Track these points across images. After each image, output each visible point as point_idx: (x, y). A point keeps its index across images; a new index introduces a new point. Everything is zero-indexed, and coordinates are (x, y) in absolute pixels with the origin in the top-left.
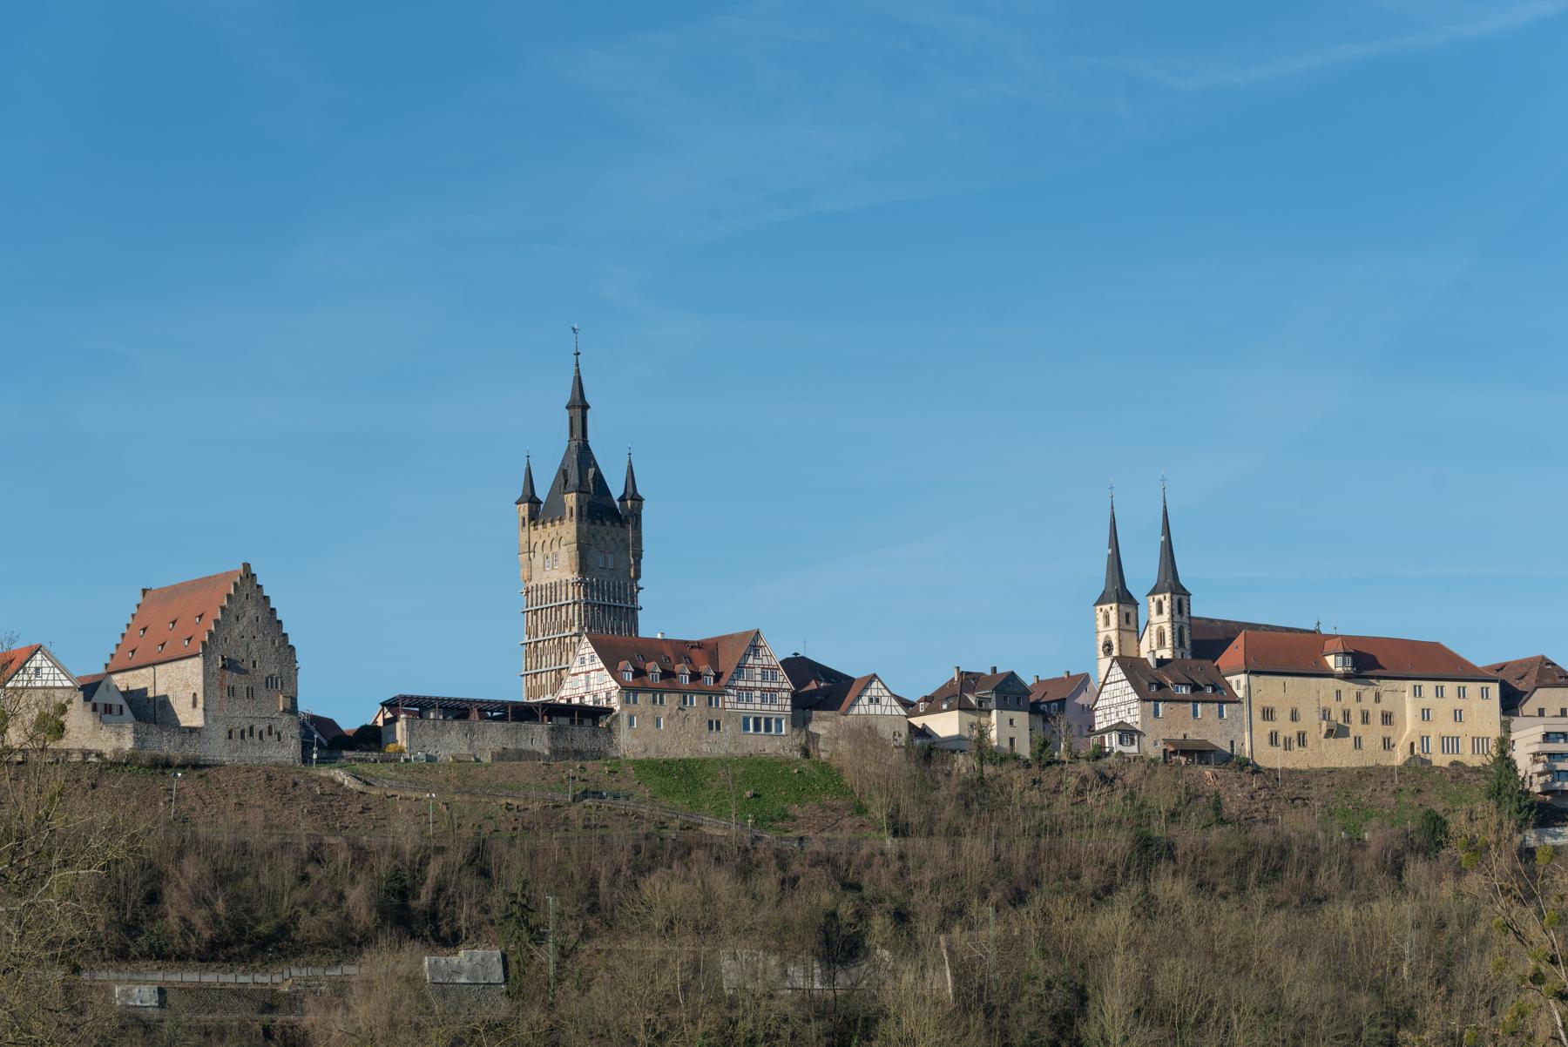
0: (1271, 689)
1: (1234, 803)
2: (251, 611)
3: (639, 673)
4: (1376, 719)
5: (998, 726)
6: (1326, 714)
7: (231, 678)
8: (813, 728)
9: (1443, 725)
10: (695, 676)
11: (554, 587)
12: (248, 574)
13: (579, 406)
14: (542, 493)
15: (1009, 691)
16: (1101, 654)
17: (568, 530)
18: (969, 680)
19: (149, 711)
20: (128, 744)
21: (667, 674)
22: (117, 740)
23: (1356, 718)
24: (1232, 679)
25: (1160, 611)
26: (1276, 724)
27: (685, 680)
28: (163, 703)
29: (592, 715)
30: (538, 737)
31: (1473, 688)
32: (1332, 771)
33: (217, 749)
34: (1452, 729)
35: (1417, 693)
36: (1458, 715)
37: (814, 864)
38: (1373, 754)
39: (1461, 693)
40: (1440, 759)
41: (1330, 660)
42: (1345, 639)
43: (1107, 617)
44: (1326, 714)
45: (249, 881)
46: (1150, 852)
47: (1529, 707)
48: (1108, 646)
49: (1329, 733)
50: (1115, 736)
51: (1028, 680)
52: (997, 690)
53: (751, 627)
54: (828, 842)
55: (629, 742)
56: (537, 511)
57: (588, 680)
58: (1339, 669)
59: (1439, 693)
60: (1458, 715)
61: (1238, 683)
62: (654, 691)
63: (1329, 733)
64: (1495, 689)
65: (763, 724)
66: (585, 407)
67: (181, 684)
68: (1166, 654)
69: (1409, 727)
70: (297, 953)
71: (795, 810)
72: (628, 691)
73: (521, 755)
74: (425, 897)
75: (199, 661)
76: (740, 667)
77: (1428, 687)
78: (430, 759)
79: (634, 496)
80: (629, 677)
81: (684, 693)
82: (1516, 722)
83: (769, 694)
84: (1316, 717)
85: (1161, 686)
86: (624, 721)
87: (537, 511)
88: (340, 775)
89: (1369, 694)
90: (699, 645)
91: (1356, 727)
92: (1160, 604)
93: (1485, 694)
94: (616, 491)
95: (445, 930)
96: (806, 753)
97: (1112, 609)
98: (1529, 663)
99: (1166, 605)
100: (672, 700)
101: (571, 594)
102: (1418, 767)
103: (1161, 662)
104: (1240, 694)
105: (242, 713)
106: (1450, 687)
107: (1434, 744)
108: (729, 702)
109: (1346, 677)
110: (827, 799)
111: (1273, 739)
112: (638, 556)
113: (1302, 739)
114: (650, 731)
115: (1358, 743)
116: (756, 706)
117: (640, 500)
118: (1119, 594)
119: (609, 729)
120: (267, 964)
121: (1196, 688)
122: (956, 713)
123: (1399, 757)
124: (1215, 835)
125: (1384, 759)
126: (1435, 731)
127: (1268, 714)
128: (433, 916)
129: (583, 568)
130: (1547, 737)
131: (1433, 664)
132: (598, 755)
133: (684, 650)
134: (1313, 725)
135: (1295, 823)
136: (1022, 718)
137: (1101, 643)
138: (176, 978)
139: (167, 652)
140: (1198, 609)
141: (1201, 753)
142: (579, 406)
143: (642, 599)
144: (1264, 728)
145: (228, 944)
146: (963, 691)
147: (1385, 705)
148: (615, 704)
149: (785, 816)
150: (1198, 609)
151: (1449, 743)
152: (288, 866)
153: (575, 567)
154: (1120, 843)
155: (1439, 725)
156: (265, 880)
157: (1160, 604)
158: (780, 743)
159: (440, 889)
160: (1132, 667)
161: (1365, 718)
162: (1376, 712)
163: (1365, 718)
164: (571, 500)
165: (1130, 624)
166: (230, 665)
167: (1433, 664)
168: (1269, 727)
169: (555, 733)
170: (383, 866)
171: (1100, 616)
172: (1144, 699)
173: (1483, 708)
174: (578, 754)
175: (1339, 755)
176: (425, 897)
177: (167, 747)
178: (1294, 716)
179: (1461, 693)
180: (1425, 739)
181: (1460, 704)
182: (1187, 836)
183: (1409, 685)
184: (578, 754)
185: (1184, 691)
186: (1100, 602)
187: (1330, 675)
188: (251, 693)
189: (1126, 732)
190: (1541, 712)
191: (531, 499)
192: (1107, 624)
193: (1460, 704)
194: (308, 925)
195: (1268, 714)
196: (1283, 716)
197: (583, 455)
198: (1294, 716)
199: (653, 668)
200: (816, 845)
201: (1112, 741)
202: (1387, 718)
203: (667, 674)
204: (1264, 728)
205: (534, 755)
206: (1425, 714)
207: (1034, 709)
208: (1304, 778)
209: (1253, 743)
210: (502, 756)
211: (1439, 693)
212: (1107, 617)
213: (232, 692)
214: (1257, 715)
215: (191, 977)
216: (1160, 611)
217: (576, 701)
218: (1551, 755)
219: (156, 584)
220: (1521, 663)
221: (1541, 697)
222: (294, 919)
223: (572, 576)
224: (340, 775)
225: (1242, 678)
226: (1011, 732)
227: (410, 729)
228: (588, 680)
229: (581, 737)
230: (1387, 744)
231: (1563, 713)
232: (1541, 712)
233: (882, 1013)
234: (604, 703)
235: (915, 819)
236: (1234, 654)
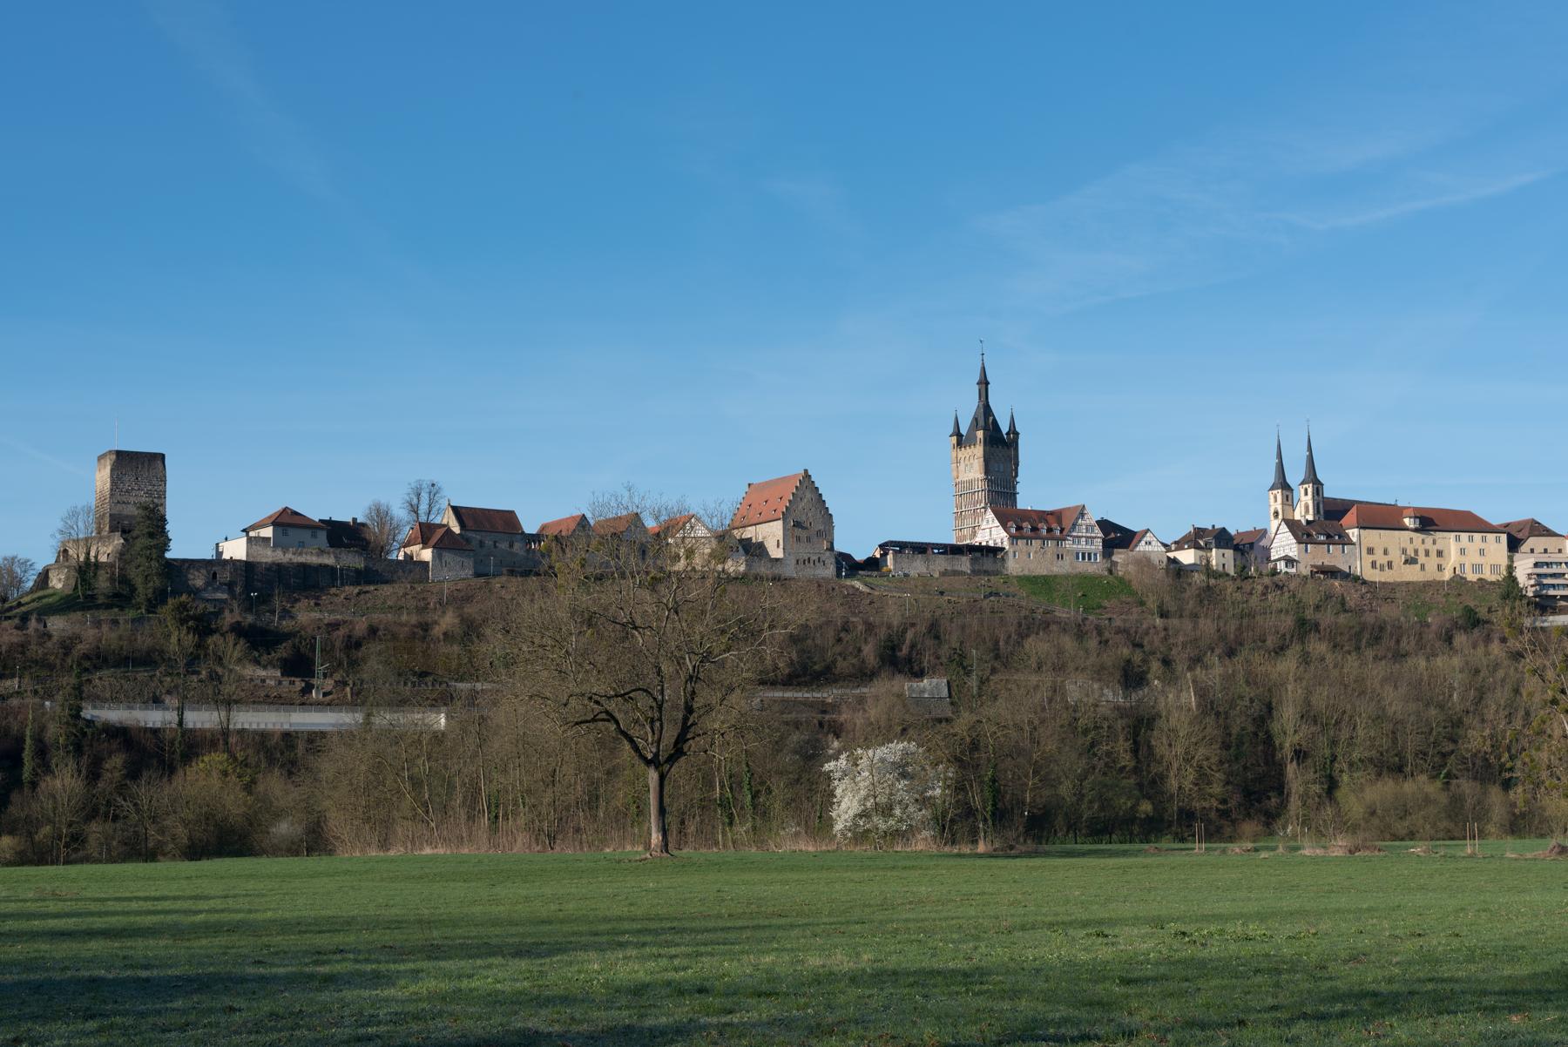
0: (1373, 537)
1: (1353, 598)
2: (808, 495)
3: (1019, 528)
4: (1433, 554)
5: (1215, 557)
6: (1404, 551)
7: (798, 531)
8: (1115, 558)
9: (1473, 558)
10: (1050, 530)
11: (971, 482)
12: (807, 475)
13: (984, 383)
14: (964, 431)
15: (1222, 538)
17: (979, 450)
18: (1199, 533)
19: (754, 550)
20: (742, 568)
21: (1035, 529)
22: (736, 565)
26: (1372, 556)
27: (1044, 532)
28: (761, 546)
29: (993, 551)
30: (964, 564)
31: (1491, 537)
32: (1408, 583)
33: (789, 570)
34: (1478, 560)
35: (1458, 539)
36: (1482, 552)
37: (1117, 633)
38: (1431, 574)
39: (1484, 540)
40: (1471, 577)
41: (1406, 521)
42: (1415, 509)
44: (1404, 551)
45: (809, 642)
46: (1305, 628)
47: (1525, 548)
48: (1276, 514)
49: (1406, 562)
50: (1283, 563)
51: (1233, 532)
52: (1215, 537)
53: (1079, 503)
54: (1124, 621)
55: (1013, 566)
56: (961, 441)
57: (991, 532)
59: (1471, 539)
60: (1482, 552)
61: (1353, 534)
62: (1027, 538)
63: (1406, 562)
64: (1504, 537)
65: (1087, 556)
66: (987, 383)
67: (771, 535)
68: (1310, 518)
69: (1453, 559)
70: (836, 681)
71: (1106, 603)
72: (1013, 538)
73: (956, 573)
74: (905, 650)
75: (779, 525)
76: (1074, 525)
77: (1464, 536)
78: (906, 575)
79: (1013, 431)
80: (1013, 530)
81: (1044, 539)
82: (1517, 556)
83: (1090, 540)
84: (1399, 553)
85: (1309, 535)
86: (1011, 555)
87: (961, 441)
88: (857, 584)
89: (1429, 540)
90: (1051, 513)
91: (1422, 559)
93: (1498, 540)
94: (1005, 429)
95: (916, 668)
96: (1110, 572)
97: (1278, 493)
98: (1525, 522)
100: (1036, 543)
101: (981, 485)
102: (1458, 581)
103: (1308, 522)
104: (1354, 539)
105: (804, 551)
106: (1477, 536)
107: (1468, 569)
108: (1068, 544)
109: (1416, 530)
110: (1123, 598)
111: (1374, 565)
112: (1017, 465)
113: (1390, 565)
114: (1025, 560)
115: (1423, 567)
116: (1083, 546)
117: (1017, 434)
118: (1283, 484)
119: (1003, 559)
120: (819, 687)
121: (1329, 536)
122: (1192, 551)
123: (1447, 575)
124: (1342, 619)
125: (1438, 577)
127: (1370, 551)
128: (909, 660)
129: (987, 472)
130: (1536, 565)
131: (1467, 523)
132: (996, 573)
133: (1043, 516)
134: (1398, 558)
135: (1387, 612)
136: (1229, 553)
138: (770, 694)
140: (1328, 493)
141: (1332, 572)
142: (984, 383)
143: (1019, 488)
145: (798, 676)
146: (1196, 539)
147: (1438, 546)
148: (1006, 545)
149: (1100, 607)
150: (1328, 493)
151: (1477, 568)
152: (831, 633)
154: (1288, 622)
155: (1471, 558)
156: (818, 642)
158: (1097, 566)
159: (913, 646)
160: (1292, 525)
161: (1427, 553)
162: (1433, 550)
163: (1427, 553)
164: (980, 434)
165: (1289, 500)
166: (797, 524)
167: (1467, 523)
168: (1371, 558)
170: (882, 633)
172: (1299, 542)
173: (1497, 548)
174: (986, 573)
175: (1412, 574)
176: (905, 650)
177: (762, 569)
178: (1386, 552)
179: (1484, 540)
180: (1462, 566)
181: (1483, 546)
182: (1327, 618)
184: (986, 573)
185: (1322, 538)
187: (1407, 529)
188: (809, 540)
189: (1289, 561)
190: (1532, 551)
191: (958, 434)
193: (1483, 546)
194: (842, 666)
197: (987, 410)
198: (1386, 552)
199: (1027, 526)
200: (1118, 623)
201: (1281, 566)
202: (1440, 553)
203: (1035, 529)
205: (962, 573)
206: (1463, 552)
207: (1236, 548)
208: (1392, 587)
209: (1360, 566)
210: (944, 574)
211: (1471, 539)
213: (798, 539)
214: (1364, 552)
215: (778, 694)
218: (1539, 575)
219: (755, 481)
220: (1519, 523)
221: (1532, 542)
222: (834, 662)
223: (982, 476)
224: (857, 584)
226: (1223, 561)
227: (895, 559)
228: (991, 532)
229: (988, 564)
230: (1440, 568)
231: (1546, 551)
232: (1532, 551)
233: (1272, 834)
235: (1172, 606)
236: (1351, 517)
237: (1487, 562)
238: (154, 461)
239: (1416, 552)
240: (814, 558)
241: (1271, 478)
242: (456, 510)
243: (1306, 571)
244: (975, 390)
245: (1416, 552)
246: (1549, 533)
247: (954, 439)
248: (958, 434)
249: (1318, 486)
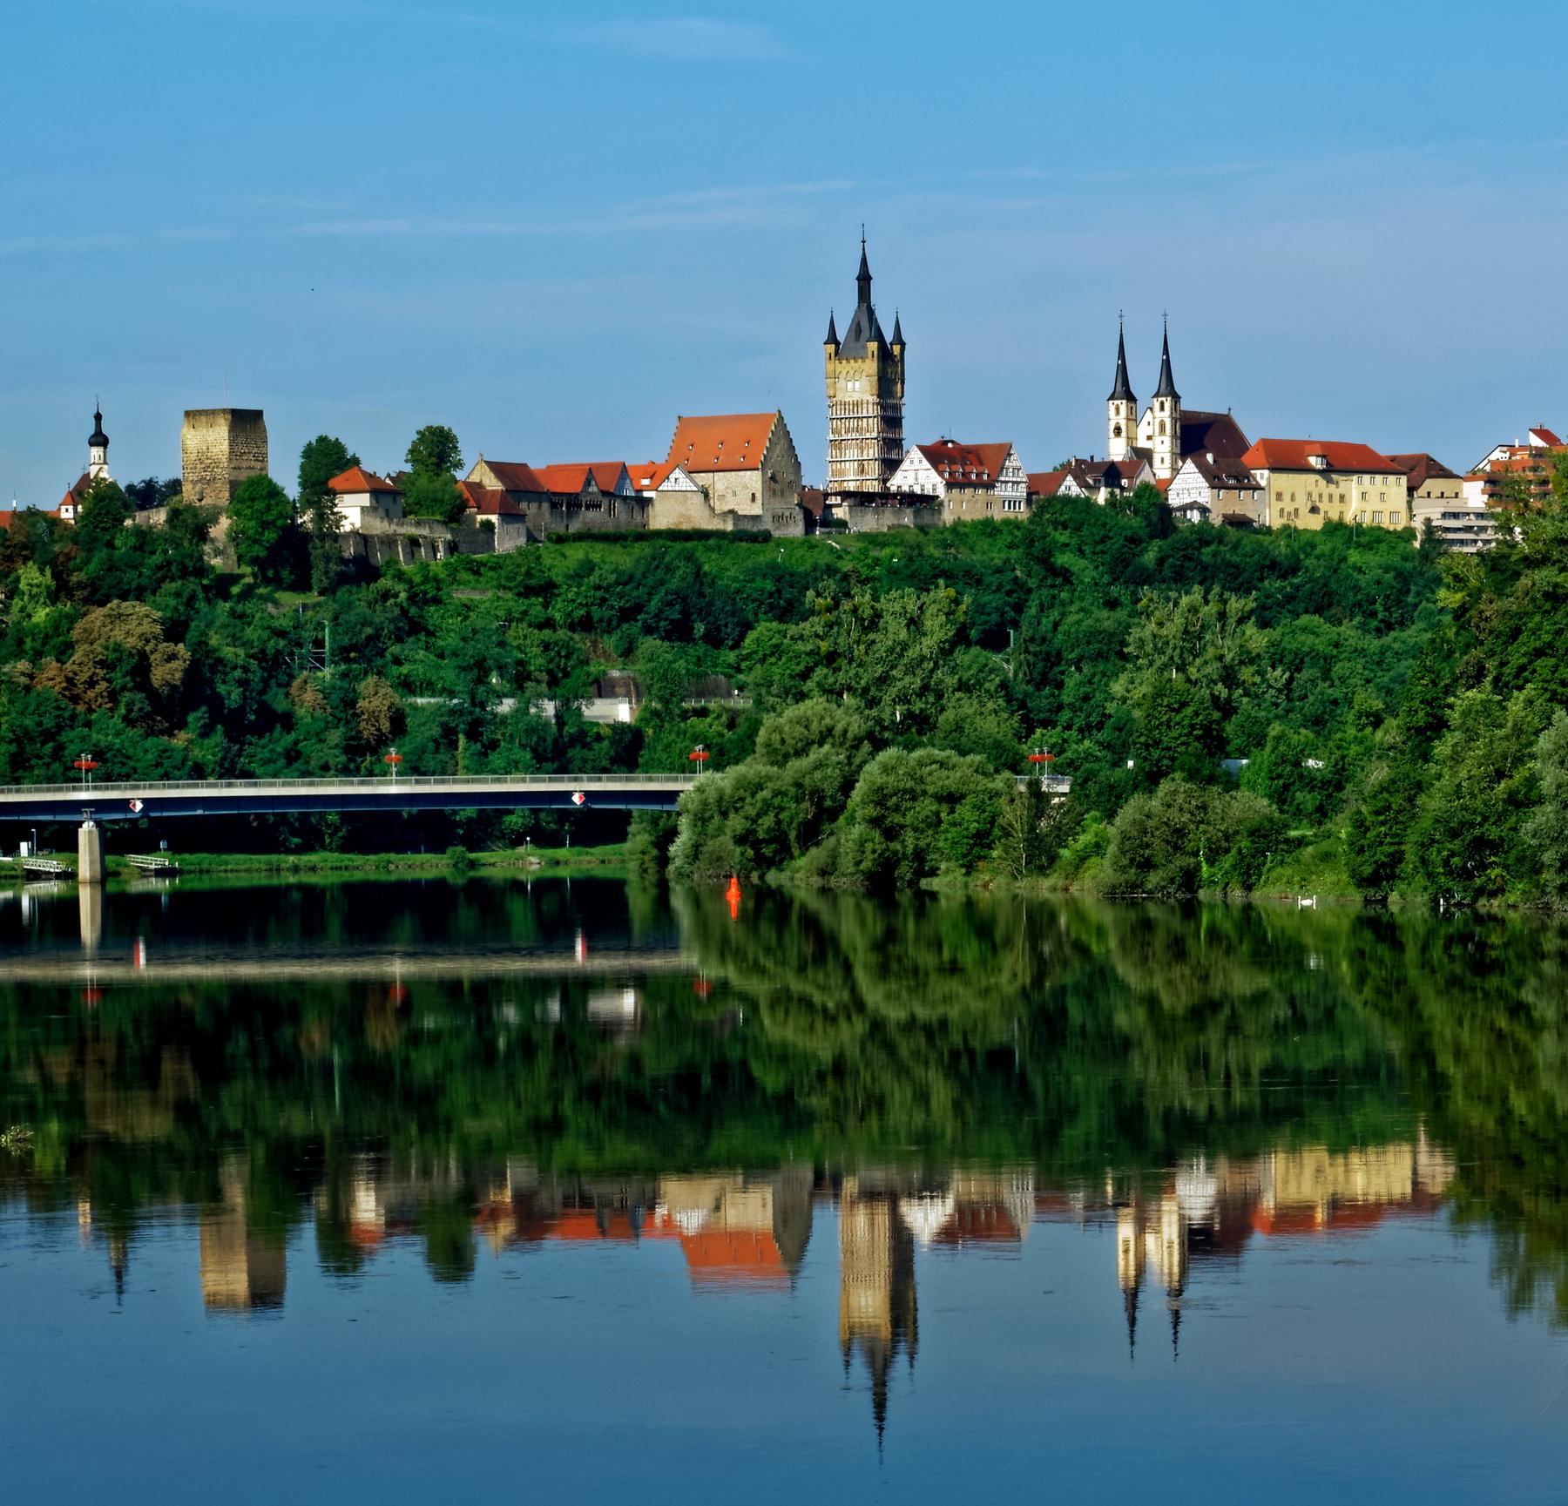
0: (1284, 481)
4: (1336, 498)
9: (1374, 504)
11: (857, 404)
13: (864, 279)
14: (841, 337)
16: (1112, 435)
23: (1325, 498)
24: (1258, 473)
25: (1162, 408)
31: (1392, 478)
34: (1378, 506)
35: (1360, 483)
39: (1385, 482)
42: (1324, 445)
43: (1117, 409)
47: (1422, 491)
48: (1118, 430)
50: (1069, 480)
55: (948, 517)
56: (838, 349)
58: (1319, 467)
61: (1262, 476)
65: (1012, 503)
72: (950, 485)
77: (1366, 478)
87: (838, 349)
92: (1162, 404)
97: (1123, 405)
99: (1167, 405)
104: (1263, 483)
105: (779, 506)
106: (1379, 478)
114: (960, 508)
126: (1369, 508)
137: (1112, 427)
139: (722, 462)
140: (1185, 405)
142: (864, 279)
143: (905, 412)
144: (1277, 506)
148: (941, 492)
153: (875, 391)
155: (1373, 501)
157: (1162, 404)
168: (1279, 505)
169: (917, 513)
171: (1112, 409)
172: (1213, 487)
178: (1293, 498)
183: (1355, 477)
185: (1232, 482)
186: (1112, 397)
191: (832, 338)
192: (1118, 413)
195: (1279, 496)
196: (1287, 497)
198: (1293, 498)
202: (1342, 498)
204: (1277, 506)
209: (1270, 516)
211: (1372, 482)
212: (1117, 409)
214: (1273, 497)
216: (1162, 408)
217: (905, 488)
219: (684, 415)
220: (1410, 458)
225: (1266, 472)
234: (929, 491)
237: (1387, 507)
238: (257, 416)
239: (1321, 496)
240: (787, 513)
241: (1109, 382)
242: (498, 469)
243: (1216, 520)
244: (854, 286)
245: (1321, 496)
246: (1445, 474)
247: (832, 347)
248: (832, 338)
249: (1176, 398)
